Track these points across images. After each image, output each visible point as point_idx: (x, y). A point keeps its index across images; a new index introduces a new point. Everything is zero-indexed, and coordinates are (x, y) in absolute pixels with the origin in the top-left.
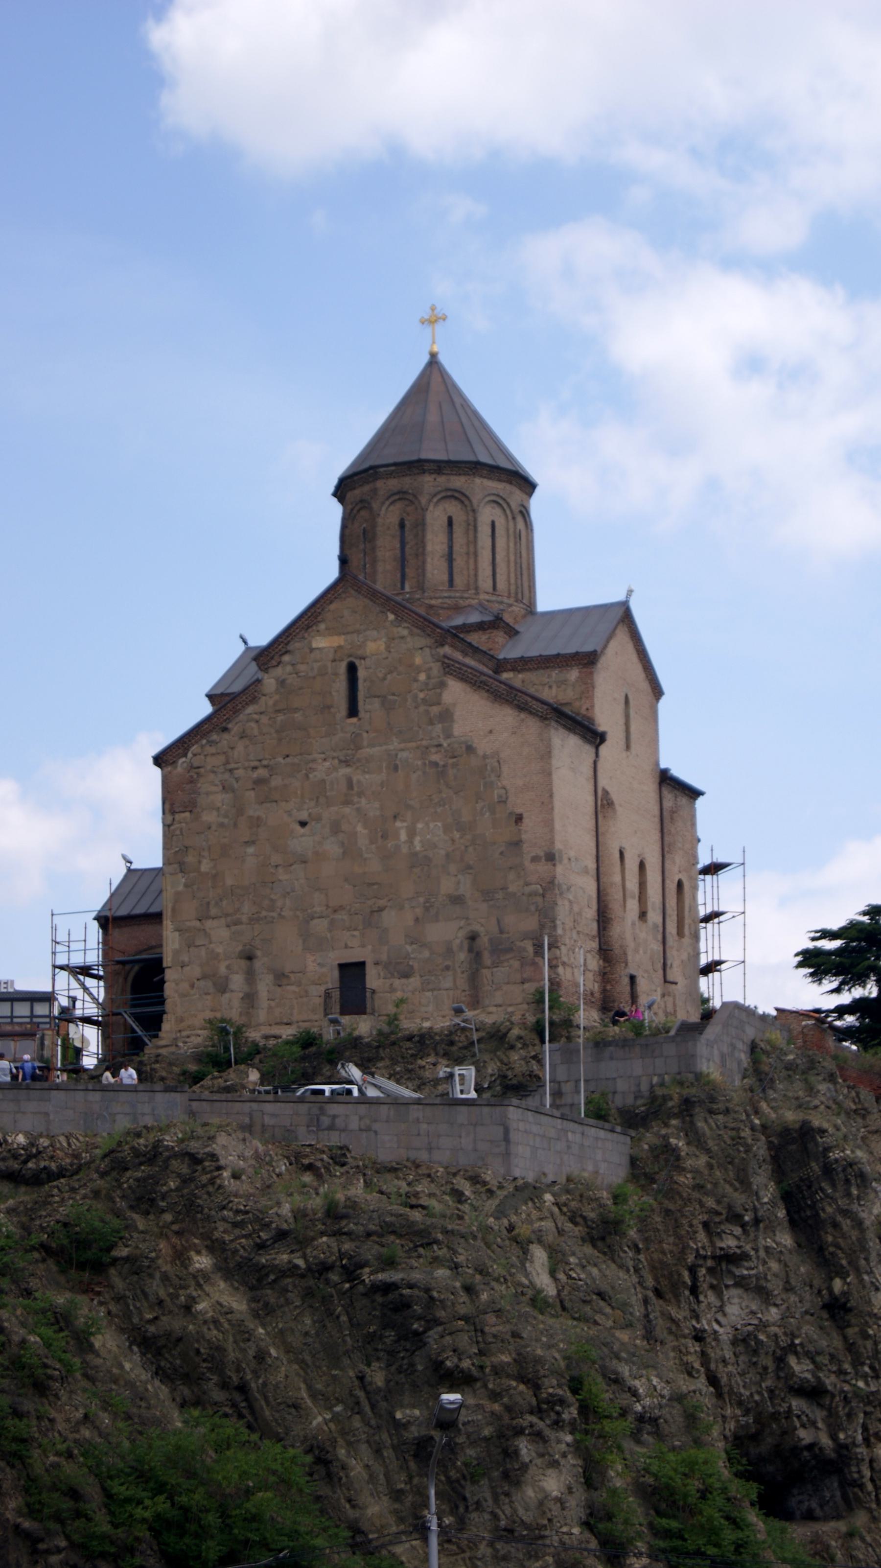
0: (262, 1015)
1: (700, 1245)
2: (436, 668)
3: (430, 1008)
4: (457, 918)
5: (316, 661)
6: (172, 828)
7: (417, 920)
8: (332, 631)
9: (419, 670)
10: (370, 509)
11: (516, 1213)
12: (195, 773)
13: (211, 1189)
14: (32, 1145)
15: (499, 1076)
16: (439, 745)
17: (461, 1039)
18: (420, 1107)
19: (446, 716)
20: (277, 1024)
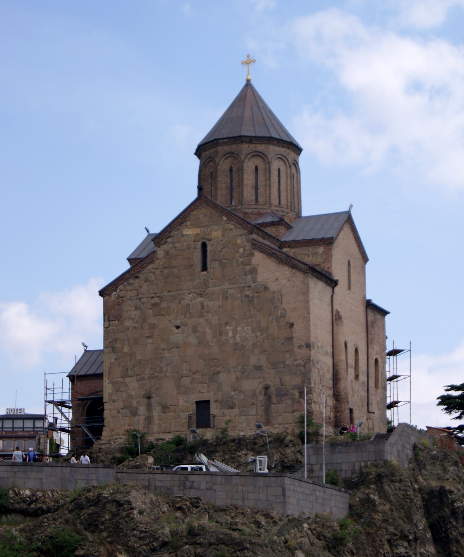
0: (155, 428)
1: (386, 551)
2: (248, 246)
3: (244, 425)
4: (258, 378)
5: (185, 241)
6: (108, 329)
7: (237, 378)
8: (193, 226)
9: (239, 247)
10: (215, 162)
11: (289, 534)
12: (121, 300)
13: (127, 519)
14: (33, 495)
15: (280, 461)
16: (250, 286)
17: (260, 442)
18: (239, 477)
19: (254, 271)
20: (163, 433)
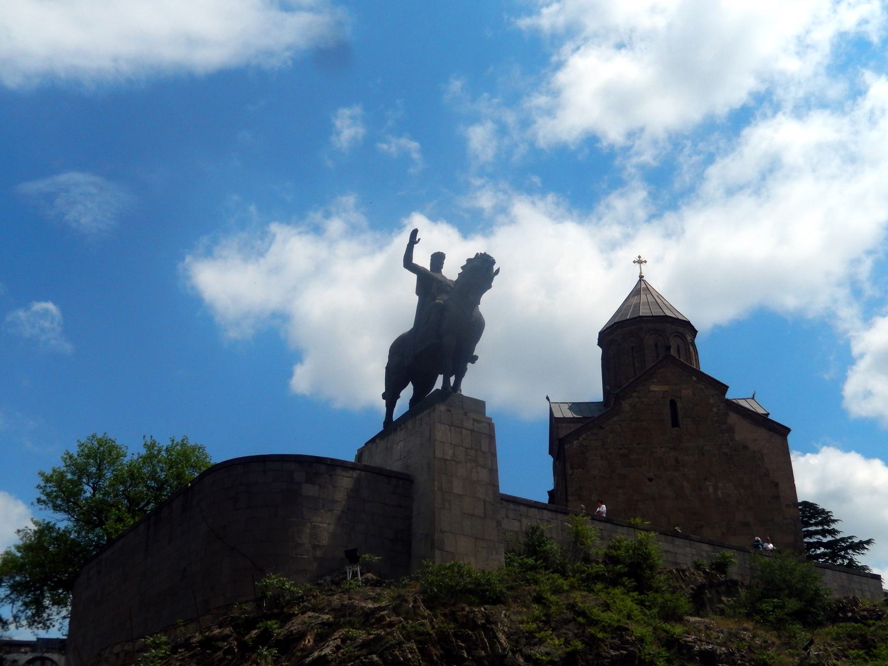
19: (731, 430)
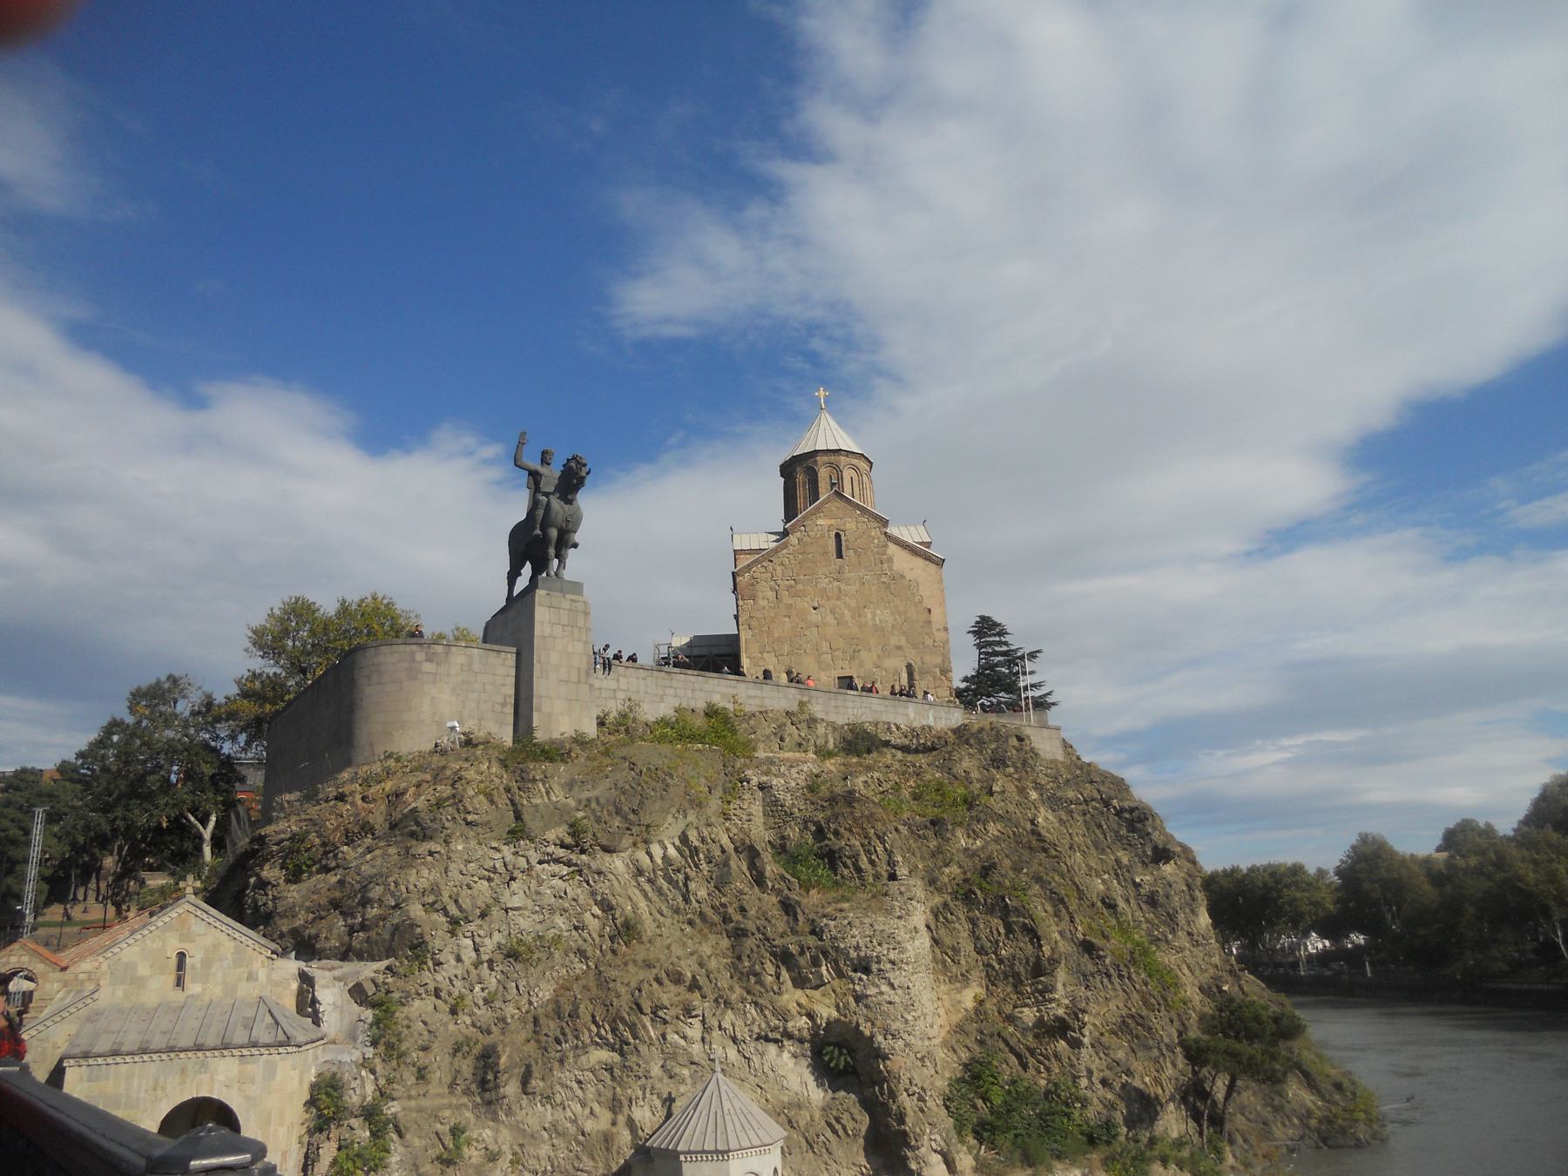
19: (890, 560)
